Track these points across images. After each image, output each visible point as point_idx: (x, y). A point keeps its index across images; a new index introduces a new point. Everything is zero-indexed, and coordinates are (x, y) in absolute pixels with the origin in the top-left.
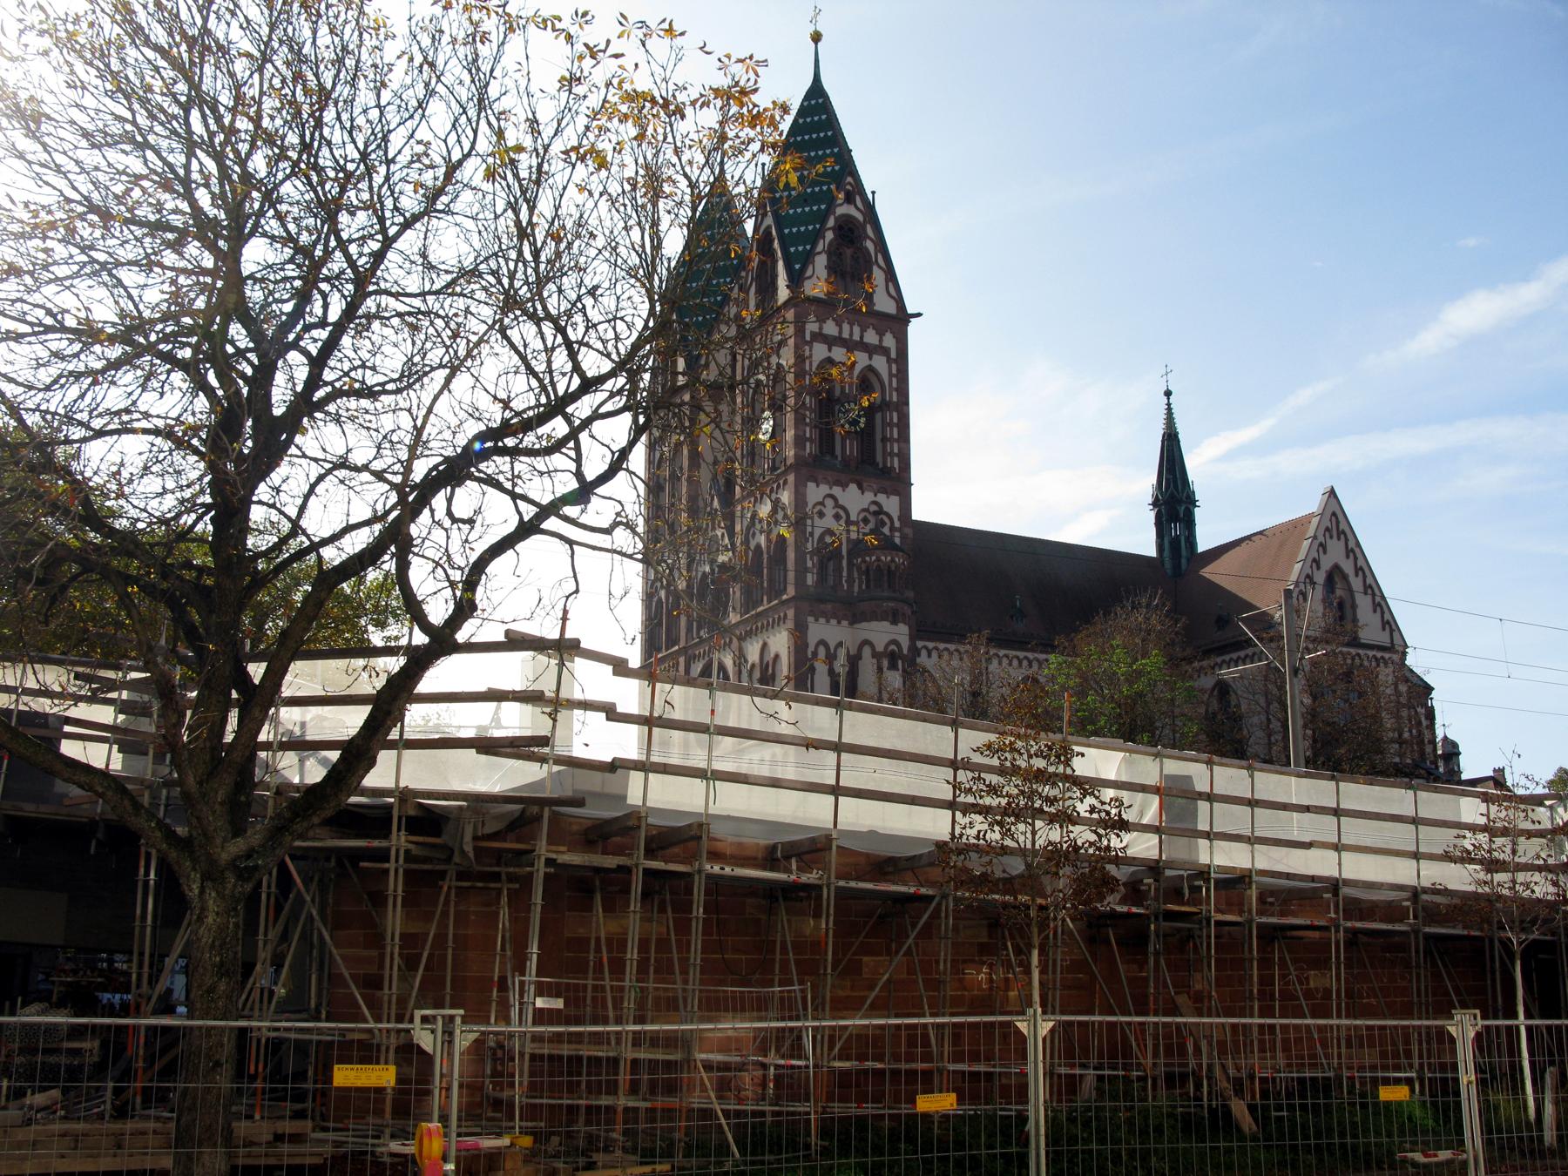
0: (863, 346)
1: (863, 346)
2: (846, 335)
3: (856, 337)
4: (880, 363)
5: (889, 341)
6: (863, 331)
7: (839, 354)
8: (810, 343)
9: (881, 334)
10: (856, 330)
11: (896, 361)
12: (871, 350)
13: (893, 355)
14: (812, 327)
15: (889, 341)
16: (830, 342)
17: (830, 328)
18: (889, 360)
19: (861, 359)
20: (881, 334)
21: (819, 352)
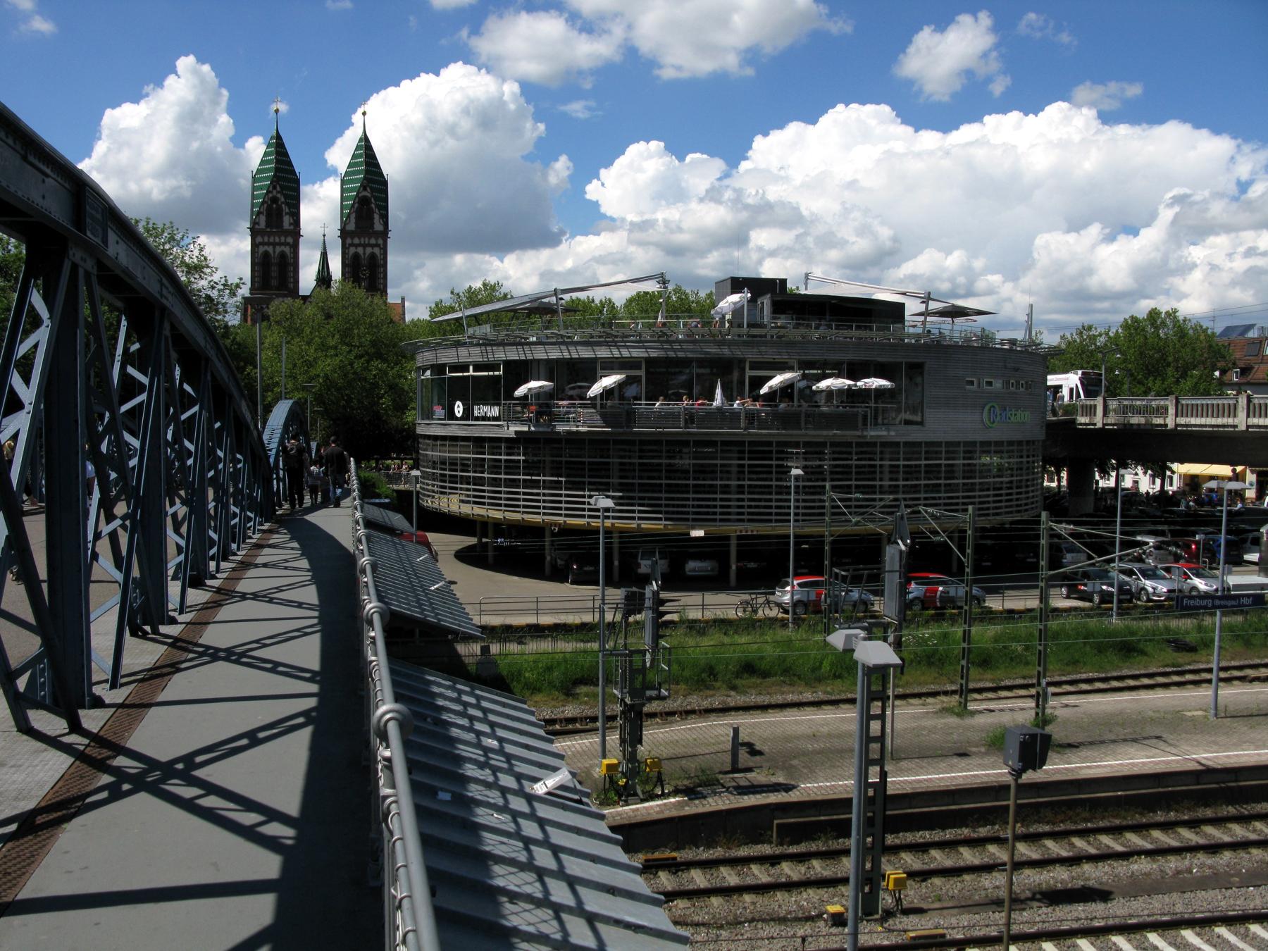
4: (377, 250)
5: (380, 241)
7: (360, 250)
12: (373, 246)
14: (349, 241)
15: (380, 241)
16: (356, 246)
17: (356, 241)
19: (369, 250)
21: (352, 250)
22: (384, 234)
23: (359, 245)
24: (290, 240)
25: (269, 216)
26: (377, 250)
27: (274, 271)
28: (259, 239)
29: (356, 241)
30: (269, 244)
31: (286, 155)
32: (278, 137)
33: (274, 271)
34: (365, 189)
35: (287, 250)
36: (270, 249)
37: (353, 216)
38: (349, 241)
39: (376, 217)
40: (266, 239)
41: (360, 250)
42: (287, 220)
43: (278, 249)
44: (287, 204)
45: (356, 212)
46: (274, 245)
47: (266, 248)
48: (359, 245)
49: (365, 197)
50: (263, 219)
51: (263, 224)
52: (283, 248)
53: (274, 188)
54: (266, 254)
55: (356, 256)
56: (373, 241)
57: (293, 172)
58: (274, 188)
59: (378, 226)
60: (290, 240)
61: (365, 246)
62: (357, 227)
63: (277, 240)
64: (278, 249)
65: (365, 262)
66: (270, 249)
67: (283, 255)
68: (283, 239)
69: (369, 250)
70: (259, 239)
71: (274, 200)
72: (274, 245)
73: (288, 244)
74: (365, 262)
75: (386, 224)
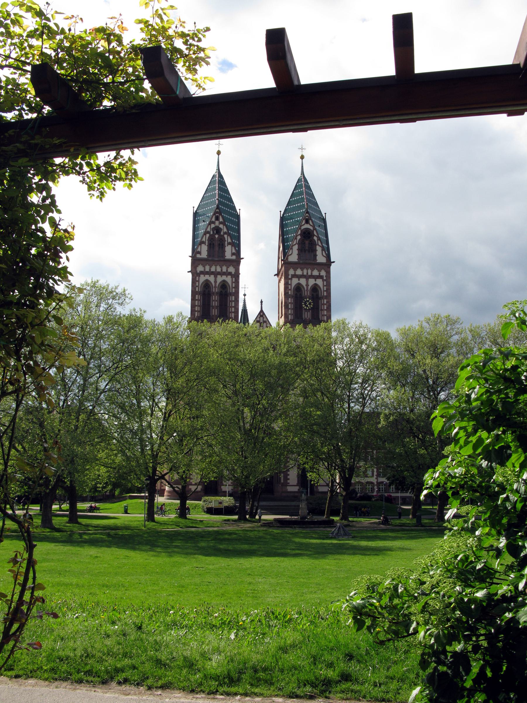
2: (305, 274)
4: (319, 282)
5: (323, 273)
6: (312, 271)
7: (303, 281)
8: (291, 279)
9: (319, 271)
11: (325, 280)
13: (325, 278)
14: (291, 272)
15: (323, 273)
16: (299, 277)
17: (299, 272)
18: (323, 280)
19: (312, 282)
21: (295, 281)
22: (329, 263)
23: (302, 276)
24: (232, 270)
25: (211, 246)
26: (319, 282)
27: (215, 301)
28: (200, 268)
29: (299, 272)
30: (210, 273)
31: (227, 191)
32: (220, 176)
33: (215, 301)
34: (307, 222)
35: (229, 279)
36: (211, 279)
37: (296, 248)
38: (291, 272)
39: (319, 249)
40: (207, 268)
41: (303, 281)
42: (229, 251)
43: (220, 279)
44: (229, 235)
45: (299, 244)
46: (216, 274)
47: (207, 277)
48: (302, 276)
49: (307, 229)
51: (204, 254)
52: (224, 278)
53: (217, 219)
54: (207, 284)
55: (298, 288)
56: (316, 273)
57: (234, 208)
58: (217, 219)
59: (321, 259)
60: (232, 270)
61: (307, 277)
62: (299, 259)
63: (219, 269)
64: (220, 279)
65: (307, 293)
66: (211, 279)
67: (224, 285)
68: (224, 269)
69: (312, 282)
70: (200, 268)
71: (217, 230)
72: (216, 274)
73: (230, 274)
74: (307, 293)
75: (328, 256)
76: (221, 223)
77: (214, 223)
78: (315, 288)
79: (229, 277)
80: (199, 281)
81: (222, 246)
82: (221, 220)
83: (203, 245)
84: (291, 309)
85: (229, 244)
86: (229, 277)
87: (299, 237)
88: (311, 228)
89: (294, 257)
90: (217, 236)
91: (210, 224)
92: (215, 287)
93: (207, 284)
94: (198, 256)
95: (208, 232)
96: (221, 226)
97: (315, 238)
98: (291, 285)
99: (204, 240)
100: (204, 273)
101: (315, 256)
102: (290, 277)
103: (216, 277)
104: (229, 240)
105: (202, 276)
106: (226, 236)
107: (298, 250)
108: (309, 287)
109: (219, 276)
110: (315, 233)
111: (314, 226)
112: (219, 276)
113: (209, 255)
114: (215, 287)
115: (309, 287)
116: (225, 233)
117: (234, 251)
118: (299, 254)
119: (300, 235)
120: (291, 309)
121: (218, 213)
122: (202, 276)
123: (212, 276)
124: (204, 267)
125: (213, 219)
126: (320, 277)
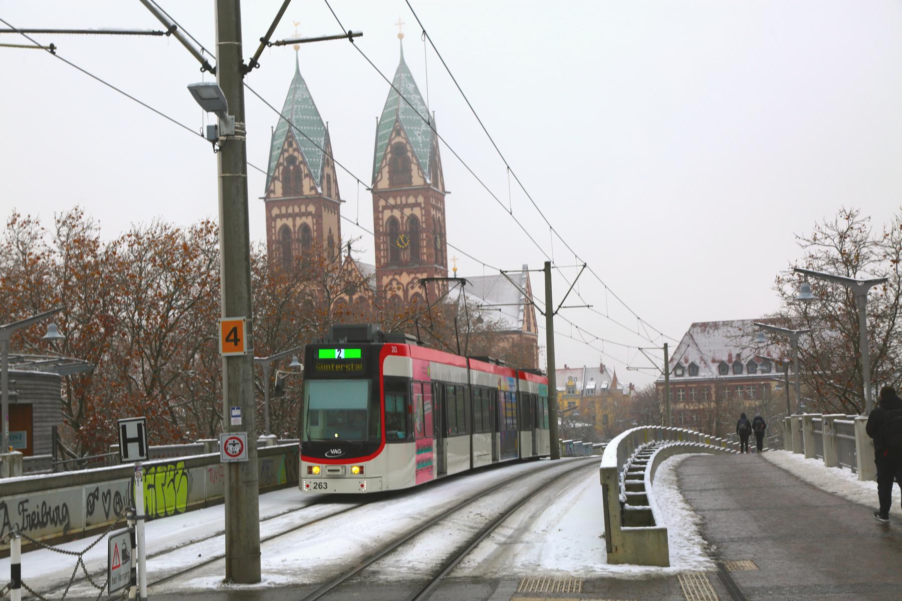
0: (407, 205)
1: (407, 205)
2: (399, 202)
3: (404, 202)
4: (417, 212)
5: (421, 199)
8: (382, 212)
9: (416, 197)
10: (404, 199)
15: (421, 199)
16: (392, 208)
17: (391, 201)
18: (421, 209)
19: (408, 212)
20: (416, 197)
21: (387, 214)
24: (312, 208)
28: (275, 211)
30: (287, 216)
34: (398, 134)
35: (309, 221)
36: (289, 222)
38: (382, 203)
39: (414, 168)
40: (284, 211)
41: (397, 213)
43: (299, 221)
45: (390, 165)
46: (294, 216)
47: (284, 221)
50: (278, 186)
52: (304, 219)
53: (290, 145)
54: (285, 229)
56: (411, 200)
58: (290, 145)
61: (401, 207)
63: (297, 210)
64: (299, 221)
65: (404, 227)
66: (289, 222)
68: (303, 209)
69: (408, 212)
70: (275, 211)
71: (291, 160)
72: (294, 216)
73: (310, 214)
74: (404, 227)
76: (295, 150)
77: (287, 151)
78: (413, 219)
79: (310, 218)
80: (275, 227)
81: (299, 180)
82: (295, 146)
83: (276, 182)
84: (384, 250)
85: (306, 176)
86: (310, 218)
87: (389, 156)
88: (404, 141)
89: (384, 184)
90: (292, 168)
91: (282, 153)
92: (295, 232)
93: (285, 229)
94: (272, 195)
95: (281, 164)
96: (296, 154)
97: (409, 154)
98: (382, 219)
99: (277, 174)
100: (280, 216)
101: (411, 177)
102: (380, 209)
103: (294, 220)
104: (306, 172)
105: (278, 220)
106: (302, 166)
107: (389, 172)
108: (405, 220)
109: (298, 219)
110: (408, 148)
111: (407, 139)
112: (298, 219)
113: (285, 193)
114: (295, 232)
115: (405, 220)
116: (301, 163)
117: (312, 184)
118: (390, 179)
119: (391, 152)
120: (384, 250)
121: (290, 139)
122: (278, 220)
123: (290, 219)
124: (280, 209)
125: (286, 147)
126: (417, 204)
